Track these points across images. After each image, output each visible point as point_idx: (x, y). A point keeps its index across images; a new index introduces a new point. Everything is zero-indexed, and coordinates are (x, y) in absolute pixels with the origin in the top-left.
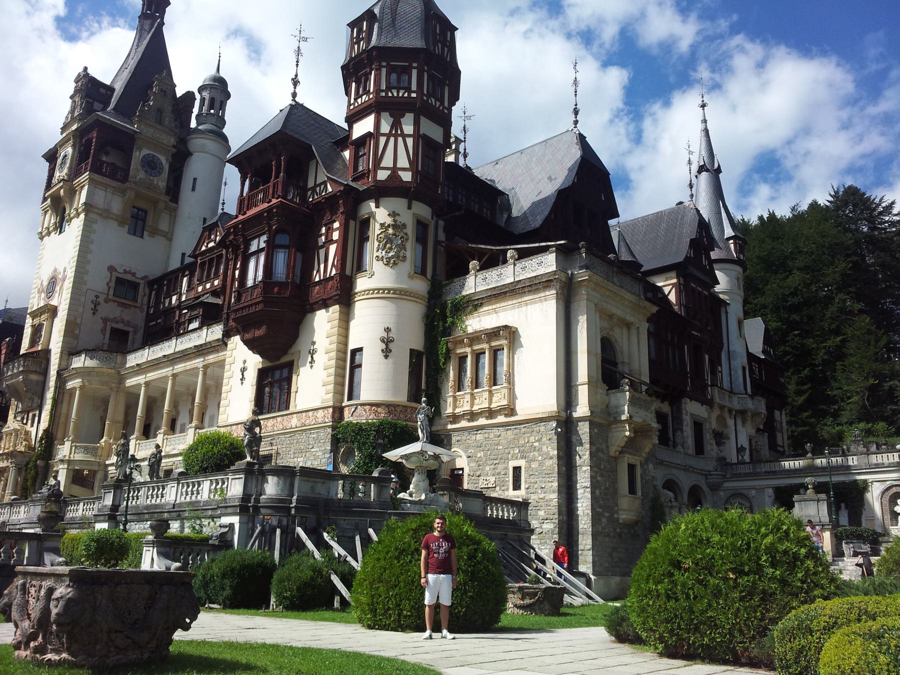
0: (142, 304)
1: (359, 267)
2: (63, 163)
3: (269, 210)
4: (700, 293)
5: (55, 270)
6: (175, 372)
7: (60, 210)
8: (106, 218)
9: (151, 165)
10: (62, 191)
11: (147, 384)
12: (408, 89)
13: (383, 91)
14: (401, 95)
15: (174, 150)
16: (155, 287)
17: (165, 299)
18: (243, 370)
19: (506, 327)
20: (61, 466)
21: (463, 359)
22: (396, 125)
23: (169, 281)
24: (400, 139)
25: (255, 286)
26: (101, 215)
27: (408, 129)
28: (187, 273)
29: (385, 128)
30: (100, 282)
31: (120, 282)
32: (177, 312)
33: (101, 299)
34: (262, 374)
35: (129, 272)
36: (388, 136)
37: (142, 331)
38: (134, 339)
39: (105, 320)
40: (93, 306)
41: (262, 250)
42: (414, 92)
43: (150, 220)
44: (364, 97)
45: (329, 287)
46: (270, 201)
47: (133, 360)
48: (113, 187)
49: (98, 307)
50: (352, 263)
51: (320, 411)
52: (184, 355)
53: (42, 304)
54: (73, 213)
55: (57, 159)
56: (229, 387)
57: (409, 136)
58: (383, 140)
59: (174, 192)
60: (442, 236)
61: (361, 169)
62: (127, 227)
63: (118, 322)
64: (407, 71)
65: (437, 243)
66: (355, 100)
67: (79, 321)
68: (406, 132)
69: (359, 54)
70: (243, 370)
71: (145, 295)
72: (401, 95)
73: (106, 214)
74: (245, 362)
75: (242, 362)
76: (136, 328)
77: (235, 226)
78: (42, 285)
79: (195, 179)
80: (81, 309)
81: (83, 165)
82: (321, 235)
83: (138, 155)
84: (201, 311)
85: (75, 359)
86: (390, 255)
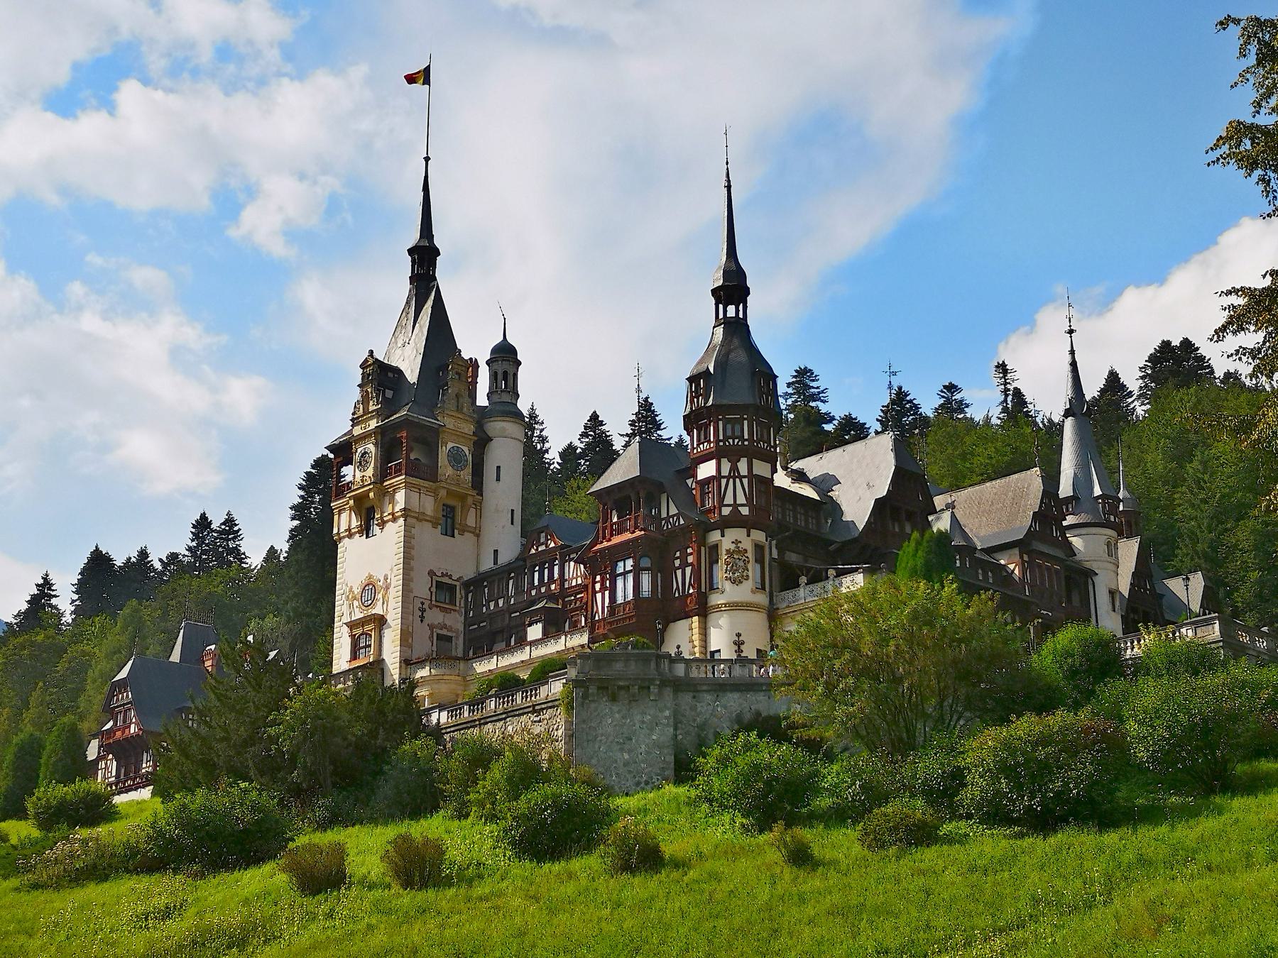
1: (712, 588)
4: (1048, 569)
5: (370, 577)
7: (364, 512)
8: (421, 520)
10: (371, 495)
12: (741, 438)
17: (488, 602)
22: (734, 468)
26: (417, 518)
27: (743, 466)
29: (725, 472)
30: (423, 588)
31: (440, 585)
35: (447, 575)
36: (728, 478)
39: (431, 627)
41: (630, 571)
43: (458, 519)
58: (724, 481)
60: (775, 555)
69: (699, 408)
73: (420, 517)
76: (457, 631)
79: (498, 468)
83: (443, 452)
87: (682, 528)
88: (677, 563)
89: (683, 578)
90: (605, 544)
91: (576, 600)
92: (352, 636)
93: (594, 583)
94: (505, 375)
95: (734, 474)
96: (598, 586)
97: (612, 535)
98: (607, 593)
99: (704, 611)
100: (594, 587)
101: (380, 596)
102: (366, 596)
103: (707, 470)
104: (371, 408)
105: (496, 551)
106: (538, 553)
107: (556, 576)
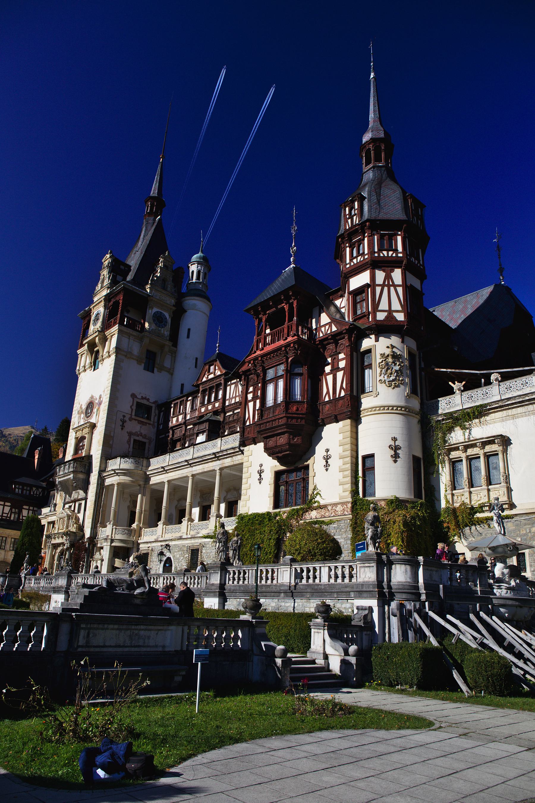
0: (154, 422)
2: (97, 319)
3: (288, 345)
6: (194, 473)
9: (158, 319)
10: (97, 339)
11: (168, 481)
12: (396, 250)
13: (376, 252)
14: (390, 255)
15: (174, 308)
16: (163, 409)
18: (260, 472)
19: (501, 435)
20: (105, 544)
21: (454, 463)
22: (388, 277)
23: (175, 405)
24: (392, 289)
25: (276, 405)
26: (126, 356)
28: (190, 398)
30: (126, 406)
31: (139, 405)
32: (184, 427)
33: (127, 419)
34: (278, 475)
35: (145, 398)
36: (383, 286)
37: (154, 441)
38: (149, 448)
39: (130, 434)
40: (121, 423)
41: (281, 377)
42: (400, 253)
43: (158, 360)
44: (359, 258)
45: (340, 405)
46: (286, 339)
47: (156, 463)
48: (134, 336)
49: (125, 424)
50: (357, 387)
51: (339, 506)
52: (203, 460)
53: (82, 422)
54: (105, 354)
55: (91, 316)
56: (248, 485)
57: (399, 286)
58: (378, 289)
59: (174, 338)
61: (359, 312)
62: (143, 365)
63: (138, 436)
64: (392, 237)
65: (421, 369)
66: (351, 260)
67: (112, 435)
68: (396, 283)
70: (260, 472)
71: (156, 414)
72: (390, 255)
74: (261, 465)
75: (259, 465)
77: (256, 359)
78: (81, 408)
79: (189, 330)
80: (113, 426)
81: (112, 320)
82: (328, 364)
83: (151, 312)
84: (206, 426)
85: (110, 462)
86: (391, 379)
88: (328, 369)
89: (333, 384)
90: (259, 352)
91: (234, 414)
92: (76, 438)
93: (247, 393)
94: (199, 272)
95: (388, 282)
96: (250, 396)
97: (265, 344)
98: (258, 401)
99: (355, 415)
100: (246, 397)
105: (182, 385)
106: (209, 381)
107: (220, 396)
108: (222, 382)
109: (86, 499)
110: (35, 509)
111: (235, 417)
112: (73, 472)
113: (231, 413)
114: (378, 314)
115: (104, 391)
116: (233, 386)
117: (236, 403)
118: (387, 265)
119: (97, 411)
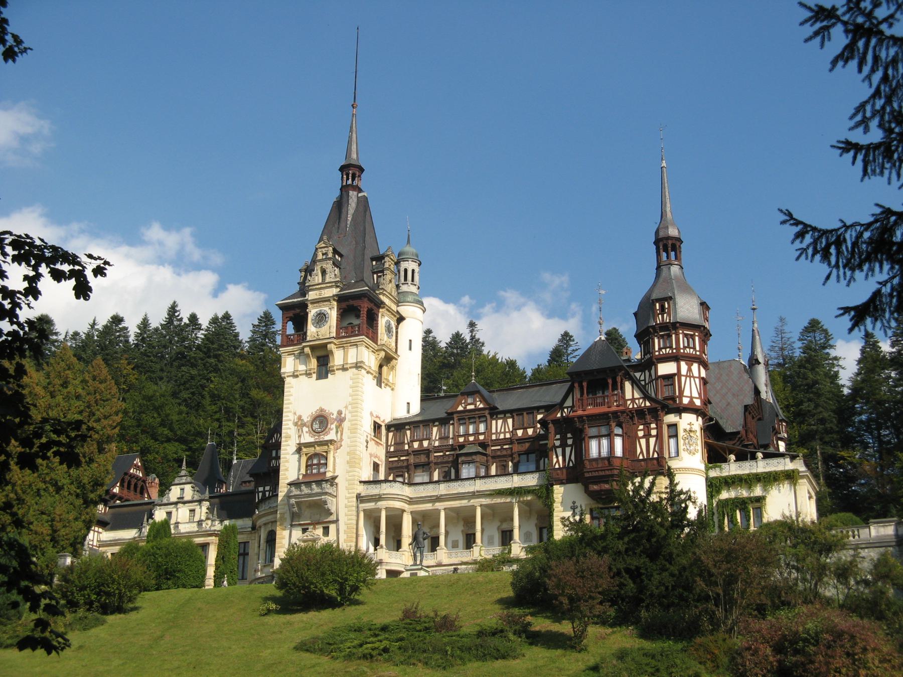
8: (368, 372)
9: (389, 329)
11: (445, 509)
12: (694, 348)
16: (393, 429)
22: (690, 370)
28: (437, 423)
31: (375, 423)
36: (686, 376)
39: (371, 455)
55: (307, 314)
58: (683, 379)
64: (693, 337)
66: (660, 349)
74: (574, 503)
87: (649, 409)
88: (641, 434)
90: (580, 412)
94: (413, 271)
95: (690, 375)
101: (333, 426)
102: (316, 426)
103: (665, 368)
104: (327, 280)
106: (465, 411)
108: (488, 417)
109: (336, 521)
110: (100, 530)
111: (504, 453)
112: (326, 493)
113: (499, 447)
114: (684, 399)
115: (346, 407)
116: (500, 422)
117: (505, 439)
118: (690, 359)
119: (337, 428)
